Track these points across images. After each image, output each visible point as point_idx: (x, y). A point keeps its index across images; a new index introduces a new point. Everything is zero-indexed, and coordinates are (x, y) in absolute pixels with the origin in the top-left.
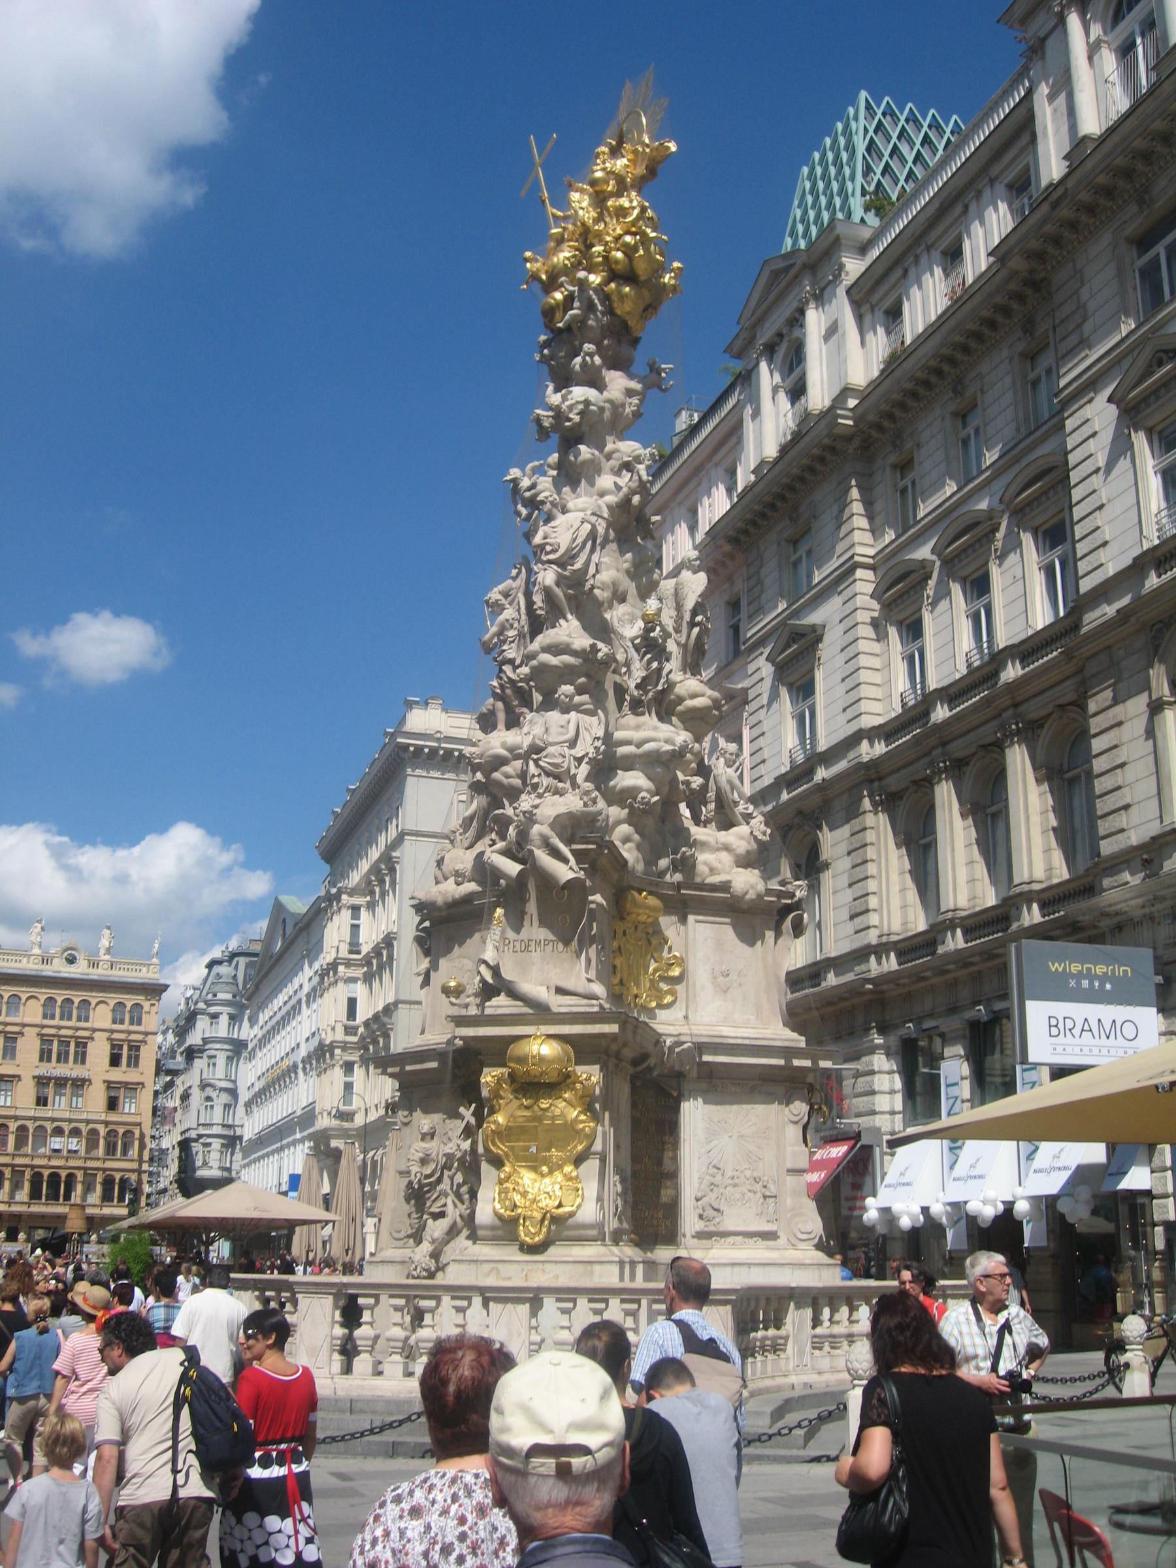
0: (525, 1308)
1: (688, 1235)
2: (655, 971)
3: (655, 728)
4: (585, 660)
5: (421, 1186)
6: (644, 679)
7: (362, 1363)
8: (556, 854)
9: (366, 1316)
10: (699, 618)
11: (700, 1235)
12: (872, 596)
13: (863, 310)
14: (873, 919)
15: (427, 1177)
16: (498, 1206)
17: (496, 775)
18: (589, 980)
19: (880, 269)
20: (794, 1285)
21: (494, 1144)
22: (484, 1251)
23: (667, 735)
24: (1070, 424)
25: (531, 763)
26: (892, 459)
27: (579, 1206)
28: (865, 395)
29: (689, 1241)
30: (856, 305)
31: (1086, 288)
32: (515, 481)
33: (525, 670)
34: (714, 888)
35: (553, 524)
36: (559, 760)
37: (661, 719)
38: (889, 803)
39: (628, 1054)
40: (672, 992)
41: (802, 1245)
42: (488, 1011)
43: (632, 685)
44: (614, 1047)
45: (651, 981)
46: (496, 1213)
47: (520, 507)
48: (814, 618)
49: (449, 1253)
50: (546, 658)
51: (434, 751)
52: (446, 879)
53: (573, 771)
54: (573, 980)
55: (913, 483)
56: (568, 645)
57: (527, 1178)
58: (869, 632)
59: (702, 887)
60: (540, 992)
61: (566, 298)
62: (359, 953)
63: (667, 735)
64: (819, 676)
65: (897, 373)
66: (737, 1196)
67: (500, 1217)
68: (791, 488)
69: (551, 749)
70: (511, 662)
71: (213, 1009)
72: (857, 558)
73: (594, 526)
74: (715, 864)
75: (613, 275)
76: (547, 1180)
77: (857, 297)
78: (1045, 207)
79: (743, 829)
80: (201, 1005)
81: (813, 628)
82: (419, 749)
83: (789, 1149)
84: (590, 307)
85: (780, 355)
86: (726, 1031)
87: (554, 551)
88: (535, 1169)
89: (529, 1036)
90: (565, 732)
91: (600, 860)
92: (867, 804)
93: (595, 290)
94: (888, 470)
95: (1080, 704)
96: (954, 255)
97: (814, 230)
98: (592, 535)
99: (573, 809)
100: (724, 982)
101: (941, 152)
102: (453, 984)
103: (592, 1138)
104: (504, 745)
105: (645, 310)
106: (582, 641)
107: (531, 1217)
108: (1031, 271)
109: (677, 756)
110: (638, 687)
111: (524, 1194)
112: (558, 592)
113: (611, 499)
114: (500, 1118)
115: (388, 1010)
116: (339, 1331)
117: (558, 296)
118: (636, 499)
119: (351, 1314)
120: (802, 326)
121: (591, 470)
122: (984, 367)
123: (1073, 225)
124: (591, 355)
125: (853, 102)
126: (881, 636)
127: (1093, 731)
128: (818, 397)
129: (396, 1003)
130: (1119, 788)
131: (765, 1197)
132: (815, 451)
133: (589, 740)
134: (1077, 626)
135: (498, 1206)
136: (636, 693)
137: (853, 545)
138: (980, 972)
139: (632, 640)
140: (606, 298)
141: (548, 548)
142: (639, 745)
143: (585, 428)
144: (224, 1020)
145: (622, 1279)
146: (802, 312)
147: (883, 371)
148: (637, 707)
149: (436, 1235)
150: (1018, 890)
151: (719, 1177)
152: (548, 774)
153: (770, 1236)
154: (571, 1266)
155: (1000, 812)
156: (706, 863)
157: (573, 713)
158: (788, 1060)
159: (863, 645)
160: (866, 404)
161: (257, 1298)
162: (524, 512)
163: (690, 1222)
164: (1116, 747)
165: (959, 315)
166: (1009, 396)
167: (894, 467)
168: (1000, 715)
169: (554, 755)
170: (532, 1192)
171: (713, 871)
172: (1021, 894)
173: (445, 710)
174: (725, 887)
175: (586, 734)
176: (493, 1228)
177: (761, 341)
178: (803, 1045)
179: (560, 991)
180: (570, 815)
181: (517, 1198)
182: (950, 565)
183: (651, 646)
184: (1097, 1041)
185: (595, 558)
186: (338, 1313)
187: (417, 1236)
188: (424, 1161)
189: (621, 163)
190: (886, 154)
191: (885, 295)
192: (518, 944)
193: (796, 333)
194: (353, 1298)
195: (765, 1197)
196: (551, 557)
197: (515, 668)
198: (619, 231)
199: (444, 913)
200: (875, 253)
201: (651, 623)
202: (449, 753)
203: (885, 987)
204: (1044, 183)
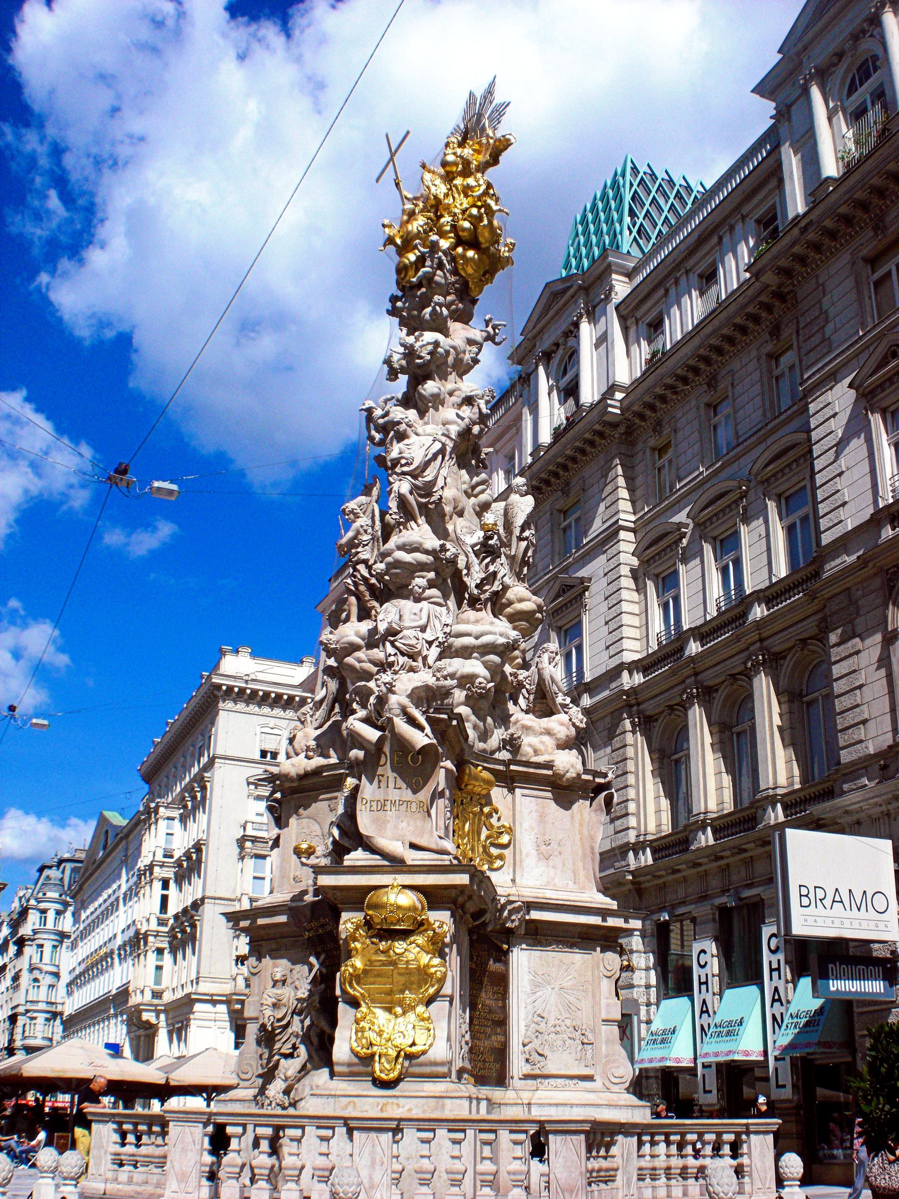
0: (387, 1137)
1: (516, 1078)
2: (488, 837)
3: (492, 623)
4: (437, 558)
5: (274, 1029)
6: (482, 580)
8: (412, 721)
9: (234, 1144)
10: (527, 533)
12: (633, 554)
13: (629, 323)
14: (632, 821)
15: (279, 1020)
16: (355, 1045)
17: (349, 660)
18: (440, 838)
19: (646, 289)
20: (623, 1121)
21: (351, 986)
22: (340, 1086)
23: (499, 630)
24: (812, 407)
25: (388, 644)
26: (652, 442)
27: (431, 1045)
28: (628, 391)
29: (516, 1083)
30: (623, 319)
31: (828, 297)
32: (369, 411)
33: (380, 567)
35: (406, 441)
36: (413, 642)
37: (495, 616)
38: (645, 724)
39: (471, 907)
40: (501, 857)
41: (615, 1088)
42: (346, 863)
43: (473, 585)
44: (461, 900)
45: (484, 847)
46: (352, 1050)
47: (373, 433)
48: (583, 573)
49: (304, 1088)
51: (242, 691)
52: (297, 754)
53: (425, 653)
54: (426, 836)
55: (670, 462)
56: (421, 544)
57: (381, 1016)
58: (631, 584)
59: (527, 764)
60: (397, 848)
61: (418, 257)
62: (171, 857)
63: (499, 630)
64: (585, 619)
65: (662, 370)
66: (560, 1043)
67: (356, 1054)
68: (565, 468)
69: (405, 632)
70: (365, 562)
71: (43, 906)
72: (621, 523)
73: (444, 445)
74: (541, 747)
75: (459, 242)
76: (401, 1020)
77: (624, 313)
78: (796, 231)
79: (563, 717)
80: (33, 902)
81: (582, 580)
82: (230, 689)
83: (604, 1002)
84: (441, 266)
85: (555, 361)
87: (407, 464)
88: (389, 1010)
89: (387, 886)
90: (417, 617)
91: (448, 732)
92: (627, 725)
93: (444, 252)
94: (648, 451)
95: (821, 637)
96: (709, 278)
97: (586, 263)
98: (442, 451)
99: (430, 684)
100: (546, 850)
101: (689, 206)
102: (304, 846)
103: (442, 981)
104: (357, 634)
105: (484, 275)
106: (432, 542)
107: (386, 1055)
108: (780, 286)
109: (512, 646)
110: (477, 586)
111: (380, 1034)
112: (411, 498)
113: (454, 430)
114: (358, 962)
115: (196, 905)
116: (209, 1159)
117: (412, 257)
118: (476, 429)
119: (219, 1142)
120: (577, 337)
121: (437, 401)
122: (736, 365)
123: (816, 247)
124: (441, 305)
126: (640, 589)
127: (833, 659)
128: (589, 393)
129: (203, 900)
130: (858, 706)
131: (583, 1044)
132: (587, 436)
133: (439, 627)
134: (817, 574)
135: (355, 1045)
136: (476, 592)
137: (617, 512)
138: (728, 865)
139: (473, 547)
140: (453, 259)
141: (403, 461)
143: (433, 367)
144: (51, 915)
145: (470, 1112)
146: (576, 325)
147: (644, 374)
148: (474, 603)
150: (764, 794)
151: (543, 1024)
152: (403, 654)
154: (423, 1101)
155: (745, 731)
156: (530, 745)
157: (424, 604)
158: (604, 920)
159: (625, 595)
160: (632, 397)
161: (115, 1131)
162: (378, 436)
163: (517, 1065)
164: (854, 671)
165: (716, 323)
166: (757, 388)
167: (653, 449)
168: (748, 649)
169: (409, 637)
170: (388, 1030)
171: (536, 752)
172: (768, 797)
173: (254, 655)
174: (548, 765)
175: (437, 623)
176: (350, 1065)
177: (539, 351)
178: (615, 907)
179: (413, 846)
180: (427, 687)
181: (373, 1036)
182: (702, 528)
183: (487, 551)
185: (444, 472)
186: (207, 1140)
187: (268, 1076)
188: (275, 1006)
189: (467, 152)
190: (647, 204)
191: (649, 311)
192: (374, 804)
193: (571, 342)
194: (220, 1128)
195: (583, 1044)
196: (406, 469)
197: (369, 568)
198: (465, 205)
199: (295, 784)
200: (639, 278)
201: (489, 532)
202: (255, 692)
203: (641, 879)
204: (791, 216)
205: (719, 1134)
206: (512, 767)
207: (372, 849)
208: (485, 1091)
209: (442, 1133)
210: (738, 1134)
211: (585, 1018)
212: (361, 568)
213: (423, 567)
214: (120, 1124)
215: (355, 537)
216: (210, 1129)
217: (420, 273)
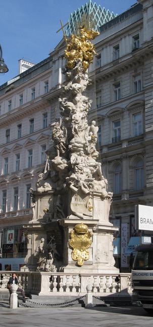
7: (55, 289)
11: (96, 263)
34: (99, 193)
59: (97, 193)
60: (81, 215)
70: (63, 142)
75: (84, 59)
88: (80, 250)
108: (139, 59)
122: (123, 76)
140: (82, 65)
153: (107, 263)
171: (97, 189)
179: (84, 215)
206: (94, 193)
207: (74, 214)
209: (92, 277)
211: (107, 251)
212: (61, 143)
213: (81, 147)
216: (50, 276)
217: (75, 68)
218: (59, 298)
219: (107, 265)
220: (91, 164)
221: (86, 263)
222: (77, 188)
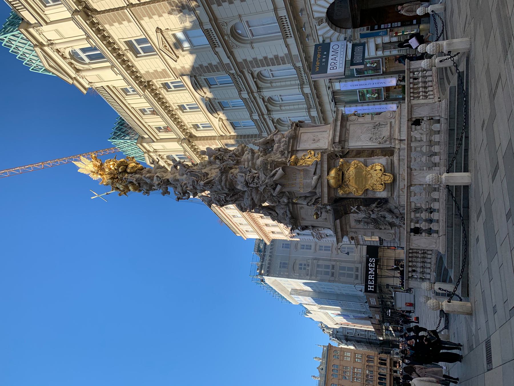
7: (434, 226)
11: (391, 143)
29: (393, 146)
50: (223, 184)
60: (315, 178)
70: (225, 197)
86: (330, 138)
116: (424, 234)
119: (417, 231)
125: (111, 143)
140: (131, 173)
142: (248, 162)
149: (391, 216)
152: (253, 181)
163: (387, 145)
171: (285, 144)
176: (388, 191)
184: (339, 56)
205: (410, 78)
208: (396, 151)
210: (410, 72)
211: (371, 125)
214: (409, 277)
215: (218, 201)
216: (412, 234)
218: (449, 225)
219: (393, 123)
220: (250, 157)
221: (390, 169)
222: (276, 185)
